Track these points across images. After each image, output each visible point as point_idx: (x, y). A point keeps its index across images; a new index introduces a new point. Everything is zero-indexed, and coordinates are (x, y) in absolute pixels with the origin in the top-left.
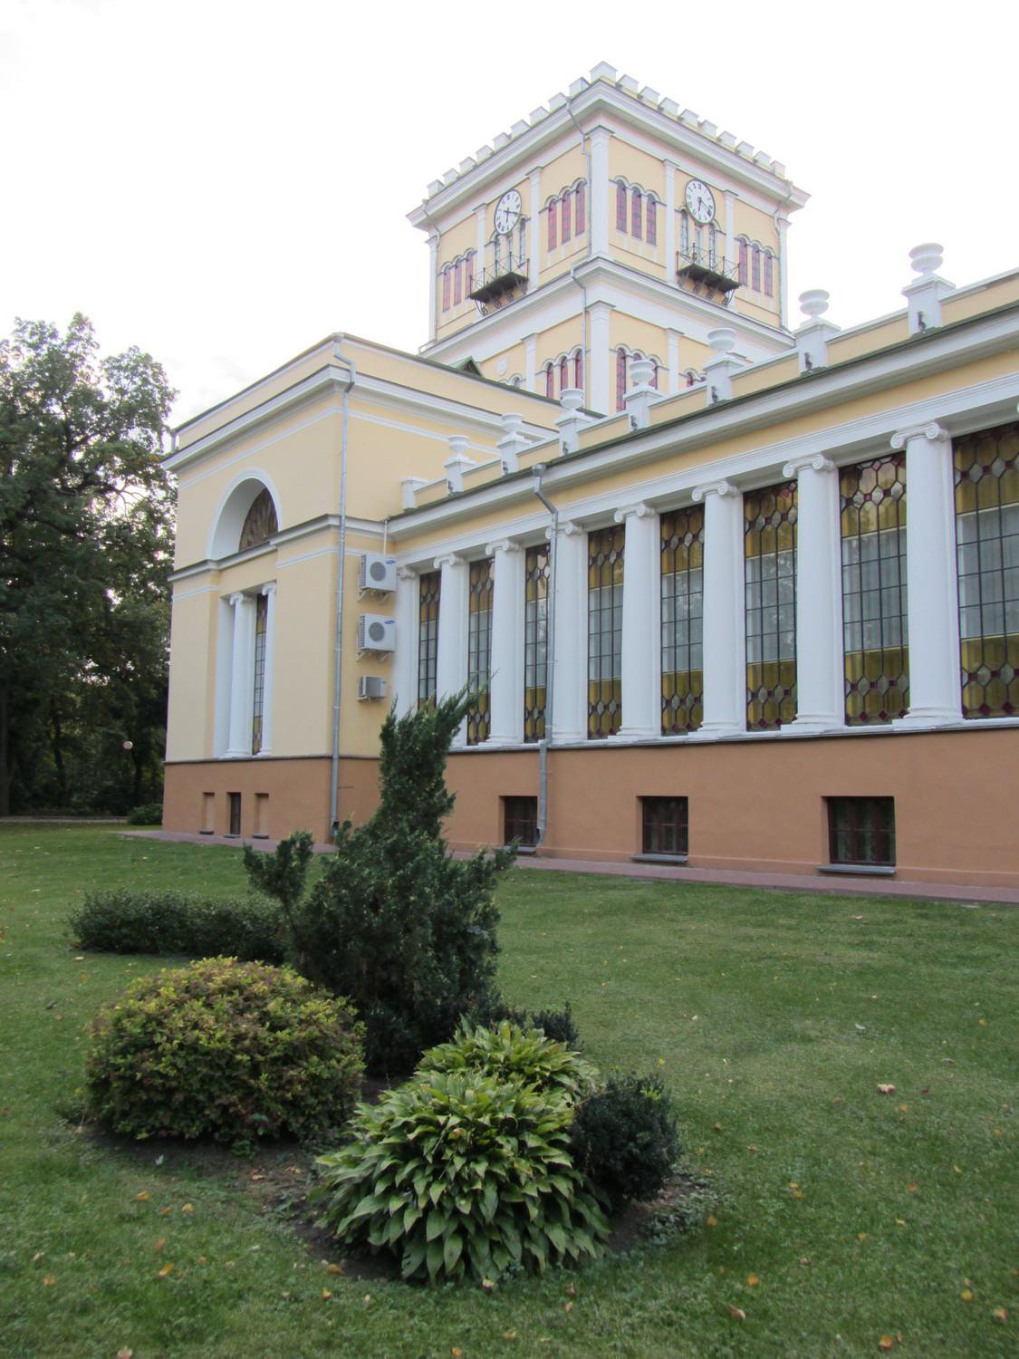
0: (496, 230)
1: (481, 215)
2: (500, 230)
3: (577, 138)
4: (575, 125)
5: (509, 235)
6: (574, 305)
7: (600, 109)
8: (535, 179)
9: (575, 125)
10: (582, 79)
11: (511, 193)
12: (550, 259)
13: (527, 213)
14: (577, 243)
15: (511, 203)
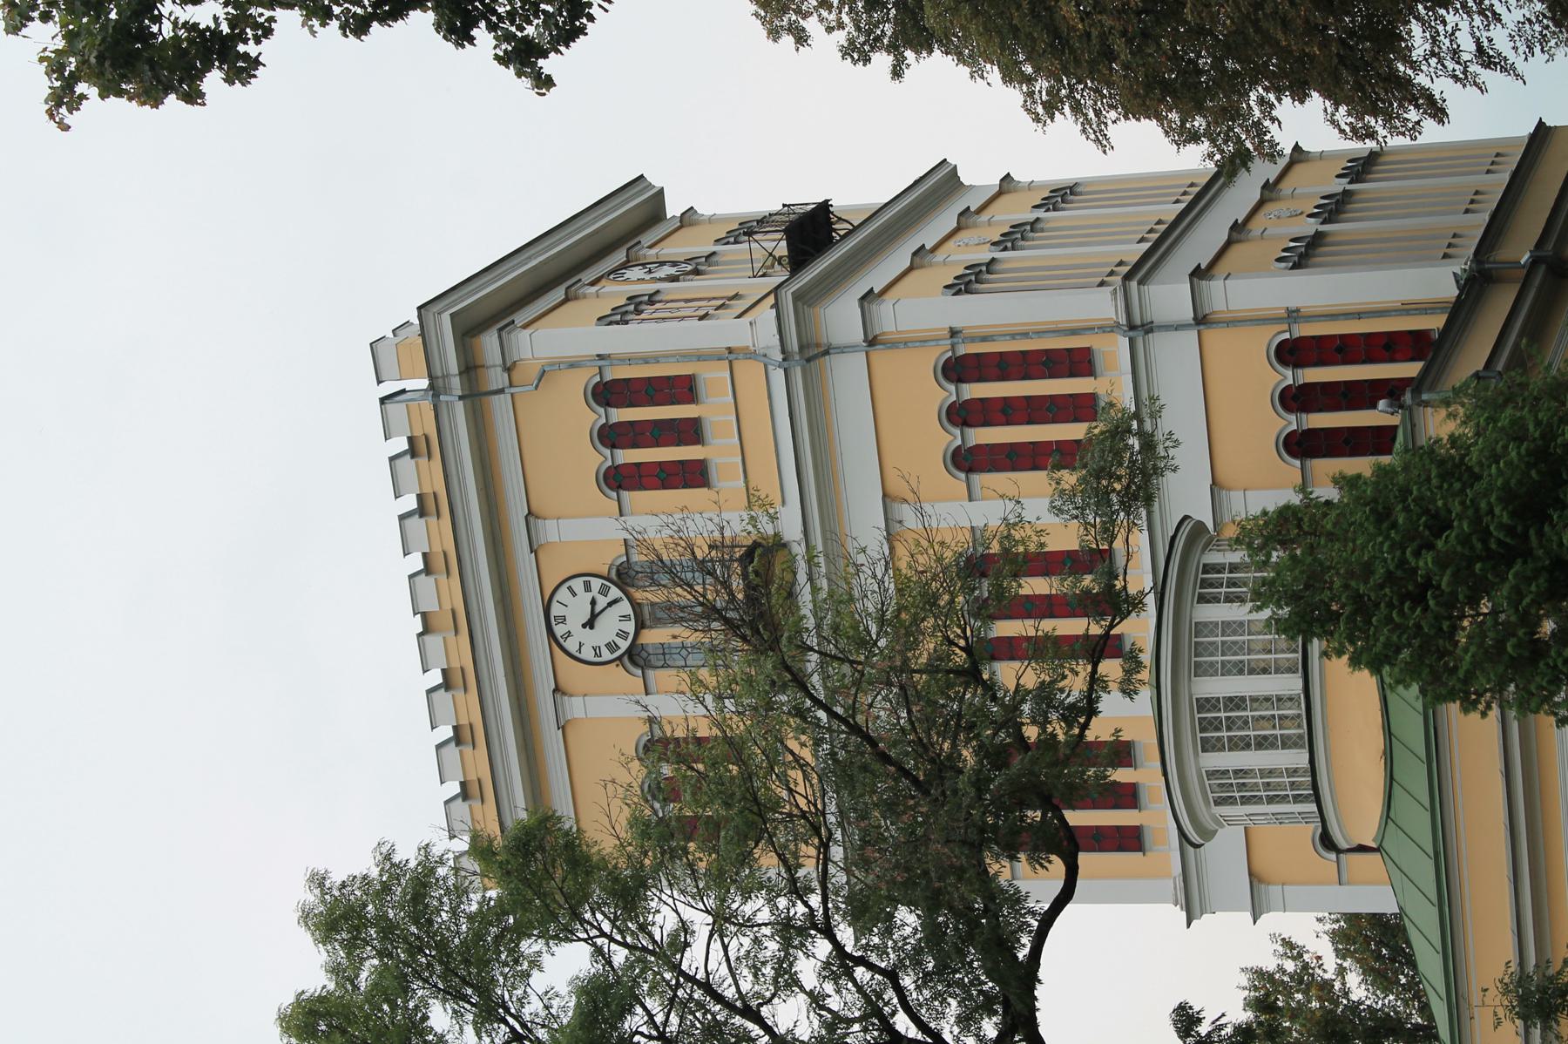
0: (620, 658)
1: (575, 707)
2: (624, 645)
3: (500, 406)
4: (475, 395)
5: (640, 626)
6: (847, 377)
7: (468, 329)
8: (550, 531)
9: (475, 395)
10: (383, 401)
11: (556, 610)
12: (727, 480)
13: (605, 560)
14: (713, 409)
15: (572, 607)
